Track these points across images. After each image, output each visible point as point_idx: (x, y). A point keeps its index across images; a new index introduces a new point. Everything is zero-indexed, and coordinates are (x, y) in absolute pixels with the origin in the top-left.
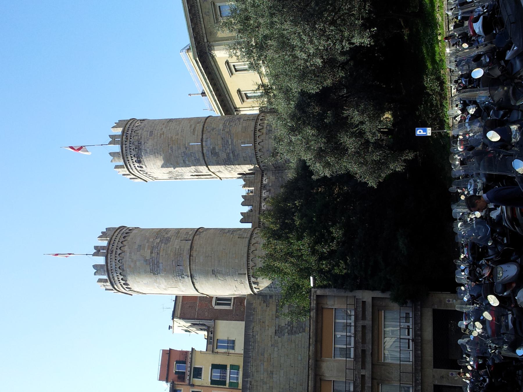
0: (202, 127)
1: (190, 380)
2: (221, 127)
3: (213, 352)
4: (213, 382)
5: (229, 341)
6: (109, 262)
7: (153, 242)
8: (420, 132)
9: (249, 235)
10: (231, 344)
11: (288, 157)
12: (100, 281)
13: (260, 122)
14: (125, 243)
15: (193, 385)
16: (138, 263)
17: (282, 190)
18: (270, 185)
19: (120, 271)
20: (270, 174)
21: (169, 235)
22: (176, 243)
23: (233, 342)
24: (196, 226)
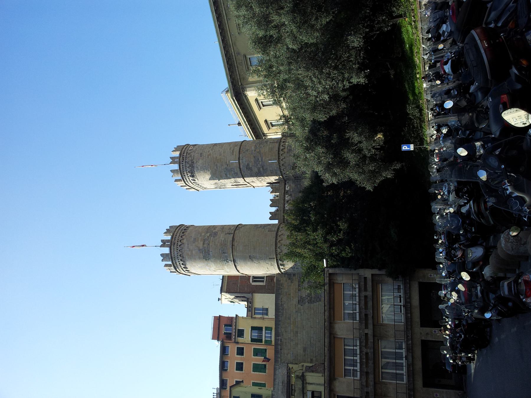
0: (238, 149)
1: (235, 339)
2: (253, 148)
3: (252, 317)
4: (253, 340)
5: (263, 309)
6: (172, 251)
7: (204, 236)
8: (405, 148)
9: (276, 229)
10: (265, 311)
11: (304, 169)
12: (166, 265)
13: (282, 144)
14: (183, 237)
15: (238, 343)
16: (194, 252)
17: (300, 195)
18: (291, 190)
19: (181, 258)
20: (291, 182)
21: (216, 231)
22: (221, 236)
23: (267, 310)
24: (237, 223)
